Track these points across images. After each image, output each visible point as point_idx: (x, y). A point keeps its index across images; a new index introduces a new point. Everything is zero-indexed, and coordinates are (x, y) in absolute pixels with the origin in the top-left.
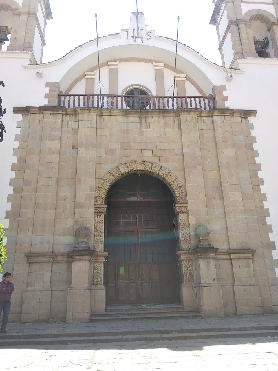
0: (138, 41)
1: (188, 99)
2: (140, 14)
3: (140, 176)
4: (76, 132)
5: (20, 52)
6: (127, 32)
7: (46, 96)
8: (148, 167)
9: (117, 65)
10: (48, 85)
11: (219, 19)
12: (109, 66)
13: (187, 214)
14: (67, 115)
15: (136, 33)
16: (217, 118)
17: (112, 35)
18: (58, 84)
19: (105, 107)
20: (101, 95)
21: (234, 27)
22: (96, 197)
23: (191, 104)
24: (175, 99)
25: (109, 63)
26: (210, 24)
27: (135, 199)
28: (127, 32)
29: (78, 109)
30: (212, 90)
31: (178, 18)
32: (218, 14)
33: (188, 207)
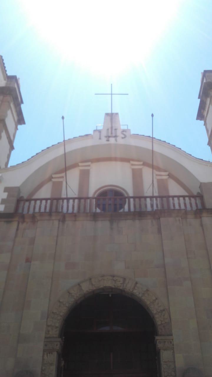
0: (112, 140)
1: (171, 199)
3: (110, 296)
4: (32, 241)
8: (119, 284)
9: (89, 166)
10: (6, 190)
11: (205, 114)
13: (172, 351)
14: (23, 222)
19: (70, 210)
22: (48, 326)
24: (154, 199)
25: (80, 164)
26: (197, 119)
27: (107, 329)
30: (200, 187)
31: (152, 115)
33: (173, 340)
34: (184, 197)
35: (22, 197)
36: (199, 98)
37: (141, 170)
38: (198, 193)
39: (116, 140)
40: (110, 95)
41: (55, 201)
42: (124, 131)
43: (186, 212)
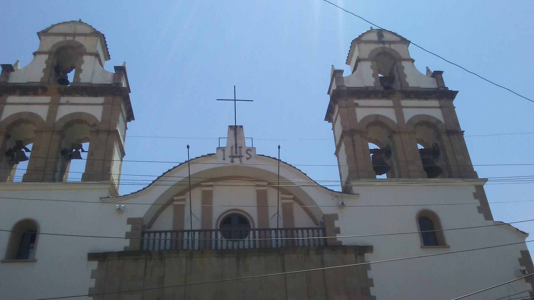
2: (239, 127)
5: (98, 183)
6: (224, 150)
7: (128, 236)
9: (211, 186)
10: (130, 221)
11: (334, 117)
12: (202, 188)
15: (234, 152)
16: (327, 256)
20: (191, 231)
21: (347, 138)
23: (300, 237)
24: (279, 231)
26: (325, 120)
28: (224, 150)
30: (323, 218)
31: (279, 147)
34: (307, 229)
35: (145, 225)
36: (329, 93)
37: (266, 190)
38: (321, 222)
39: (241, 161)
40: (234, 101)
41: (180, 234)
42: (249, 150)
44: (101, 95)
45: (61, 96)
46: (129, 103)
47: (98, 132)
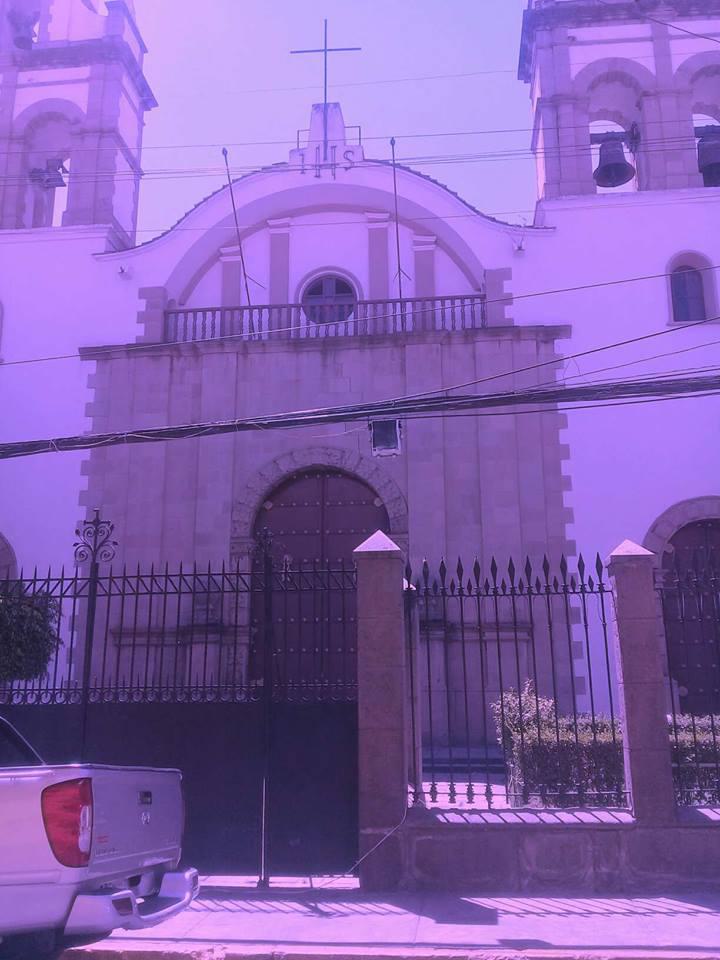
2: (331, 106)
4: (198, 391)
5: (85, 227)
6: (303, 155)
8: (334, 461)
11: (531, 71)
14: (180, 356)
17: (270, 168)
18: (163, 290)
28: (303, 155)
29: (198, 345)
32: (529, 62)
34: (453, 299)
35: (172, 300)
37: (386, 230)
39: (334, 175)
43: (449, 336)
44: (86, 62)
45: (21, 70)
46: (139, 73)
47: (83, 133)
